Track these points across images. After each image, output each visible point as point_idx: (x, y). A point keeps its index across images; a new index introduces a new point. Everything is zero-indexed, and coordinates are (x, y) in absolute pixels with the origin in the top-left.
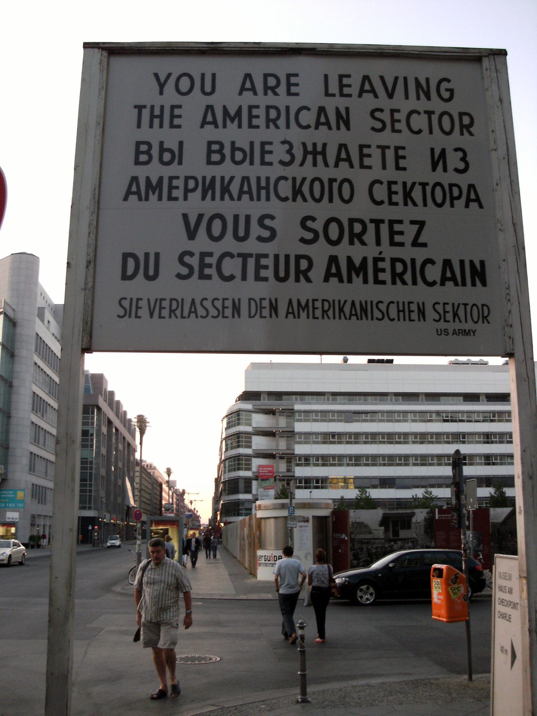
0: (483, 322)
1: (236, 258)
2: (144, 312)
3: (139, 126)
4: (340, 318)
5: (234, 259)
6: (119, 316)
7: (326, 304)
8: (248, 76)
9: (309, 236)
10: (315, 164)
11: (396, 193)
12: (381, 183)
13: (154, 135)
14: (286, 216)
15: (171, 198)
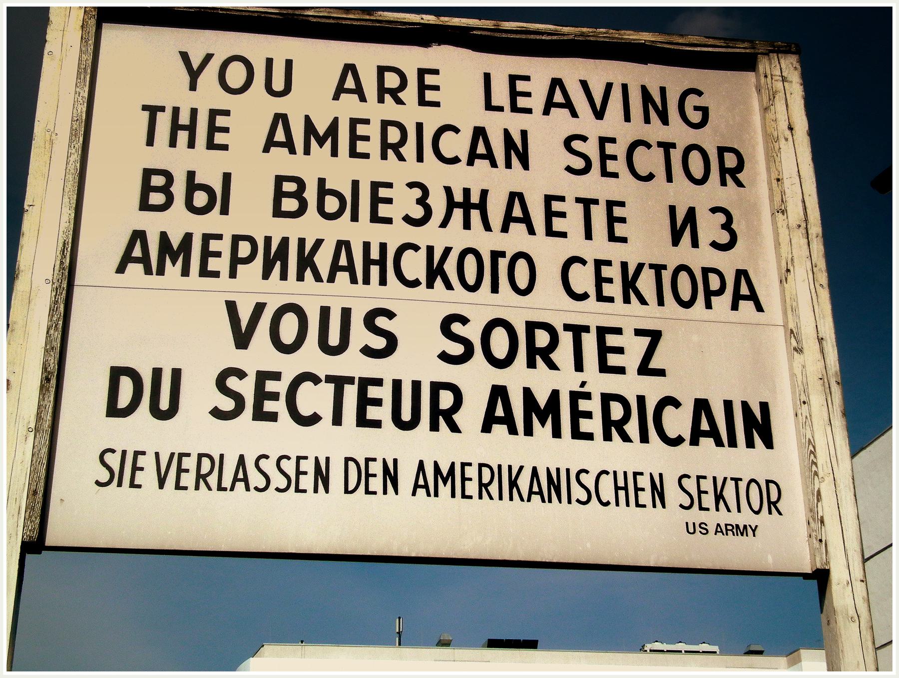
0: (770, 513)
1: (323, 383)
2: (147, 477)
3: (150, 142)
4: (511, 499)
6: (98, 483)
7: (486, 472)
8: (350, 68)
9: (457, 349)
10: (467, 225)
11: (610, 281)
12: (583, 262)
13: (179, 160)
15: (204, 272)
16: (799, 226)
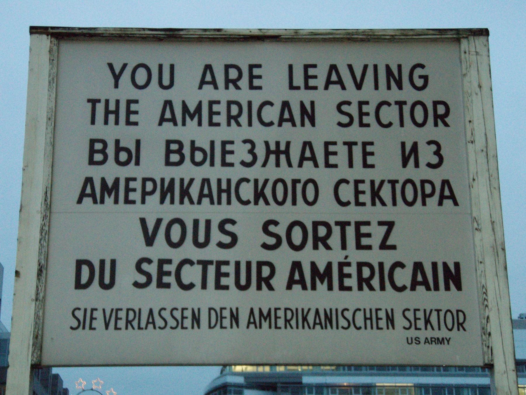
0: (459, 330)
2: (99, 323)
3: (93, 122)
4: (303, 327)
5: (193, 266)
6: (72, 328)
8: (208, 68)
9: (272, 241)
10: (278, 165)
11: (363, 192)
12: (347, 182)
14: (248, 220)
15: (127, 201)
16: (482, 151)
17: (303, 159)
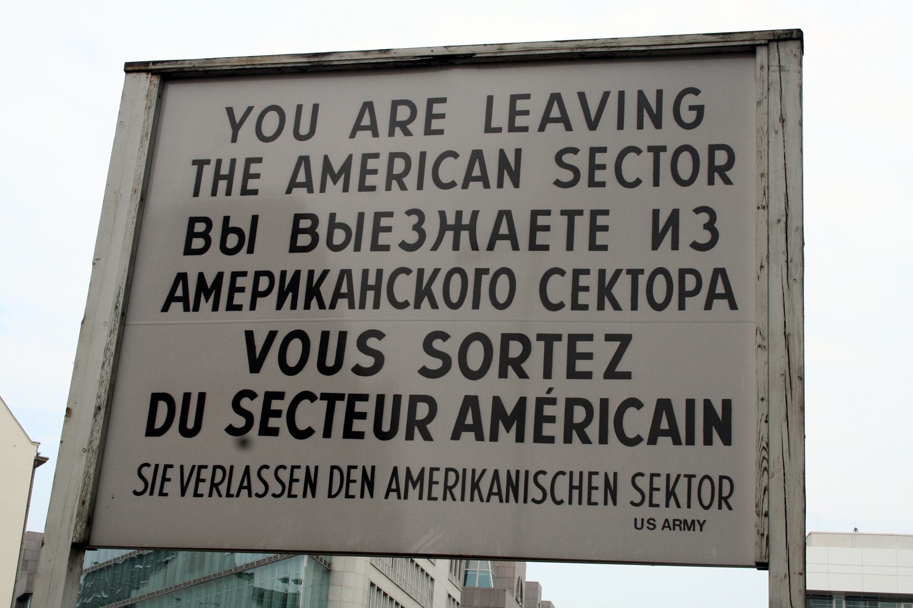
0: (720, 507)
2: (173, 487)
4: (472, 499)
6: (135, 493)
7: (452, 475)
8: (368, 106)
9: (435, 364)
10: (456, 247)
11: (586, 289)
12: (562, 273)
13: (215, 207)
15: (231, 307)
17: (496, 236)
